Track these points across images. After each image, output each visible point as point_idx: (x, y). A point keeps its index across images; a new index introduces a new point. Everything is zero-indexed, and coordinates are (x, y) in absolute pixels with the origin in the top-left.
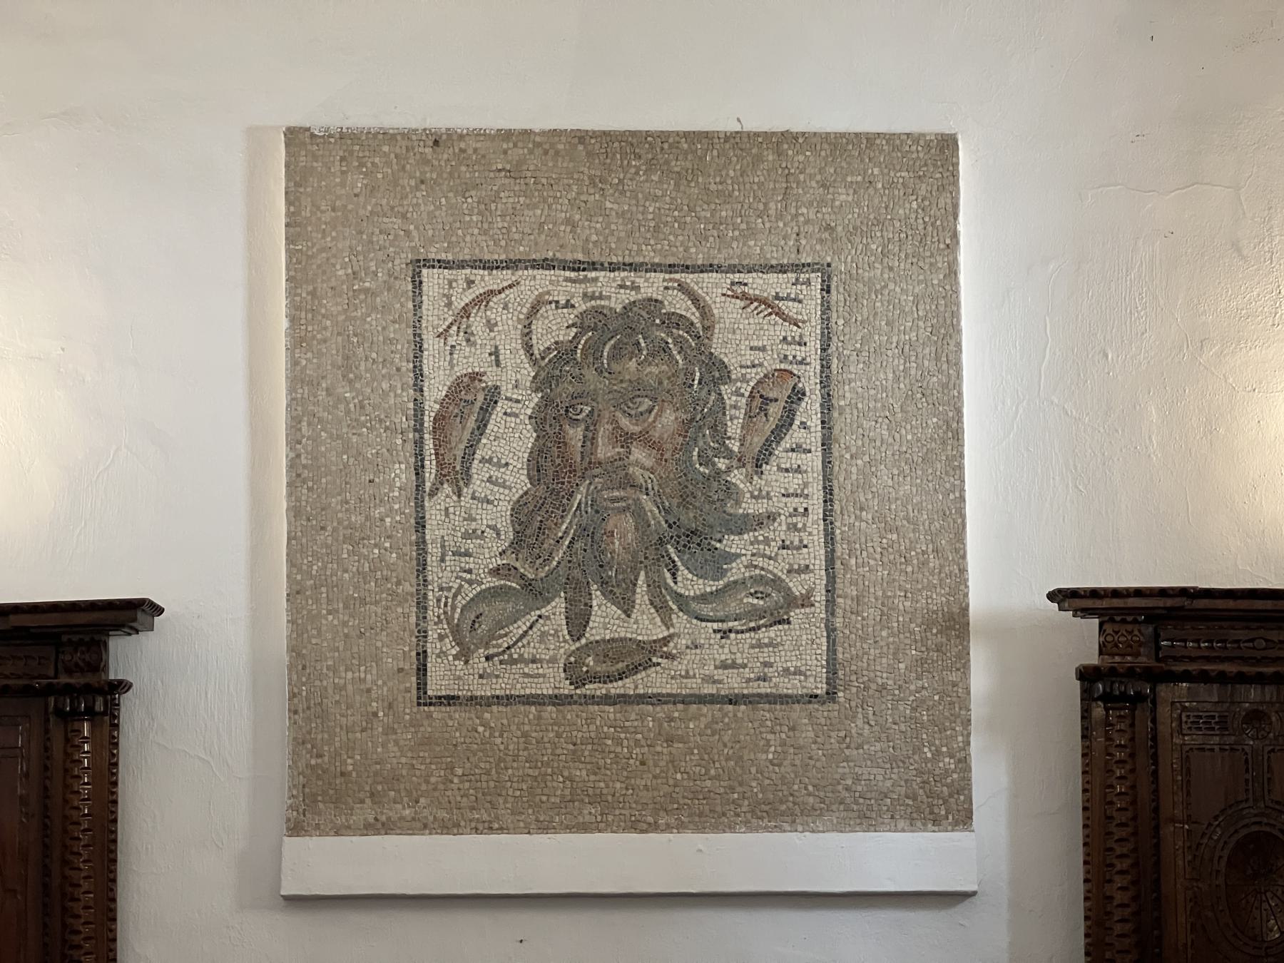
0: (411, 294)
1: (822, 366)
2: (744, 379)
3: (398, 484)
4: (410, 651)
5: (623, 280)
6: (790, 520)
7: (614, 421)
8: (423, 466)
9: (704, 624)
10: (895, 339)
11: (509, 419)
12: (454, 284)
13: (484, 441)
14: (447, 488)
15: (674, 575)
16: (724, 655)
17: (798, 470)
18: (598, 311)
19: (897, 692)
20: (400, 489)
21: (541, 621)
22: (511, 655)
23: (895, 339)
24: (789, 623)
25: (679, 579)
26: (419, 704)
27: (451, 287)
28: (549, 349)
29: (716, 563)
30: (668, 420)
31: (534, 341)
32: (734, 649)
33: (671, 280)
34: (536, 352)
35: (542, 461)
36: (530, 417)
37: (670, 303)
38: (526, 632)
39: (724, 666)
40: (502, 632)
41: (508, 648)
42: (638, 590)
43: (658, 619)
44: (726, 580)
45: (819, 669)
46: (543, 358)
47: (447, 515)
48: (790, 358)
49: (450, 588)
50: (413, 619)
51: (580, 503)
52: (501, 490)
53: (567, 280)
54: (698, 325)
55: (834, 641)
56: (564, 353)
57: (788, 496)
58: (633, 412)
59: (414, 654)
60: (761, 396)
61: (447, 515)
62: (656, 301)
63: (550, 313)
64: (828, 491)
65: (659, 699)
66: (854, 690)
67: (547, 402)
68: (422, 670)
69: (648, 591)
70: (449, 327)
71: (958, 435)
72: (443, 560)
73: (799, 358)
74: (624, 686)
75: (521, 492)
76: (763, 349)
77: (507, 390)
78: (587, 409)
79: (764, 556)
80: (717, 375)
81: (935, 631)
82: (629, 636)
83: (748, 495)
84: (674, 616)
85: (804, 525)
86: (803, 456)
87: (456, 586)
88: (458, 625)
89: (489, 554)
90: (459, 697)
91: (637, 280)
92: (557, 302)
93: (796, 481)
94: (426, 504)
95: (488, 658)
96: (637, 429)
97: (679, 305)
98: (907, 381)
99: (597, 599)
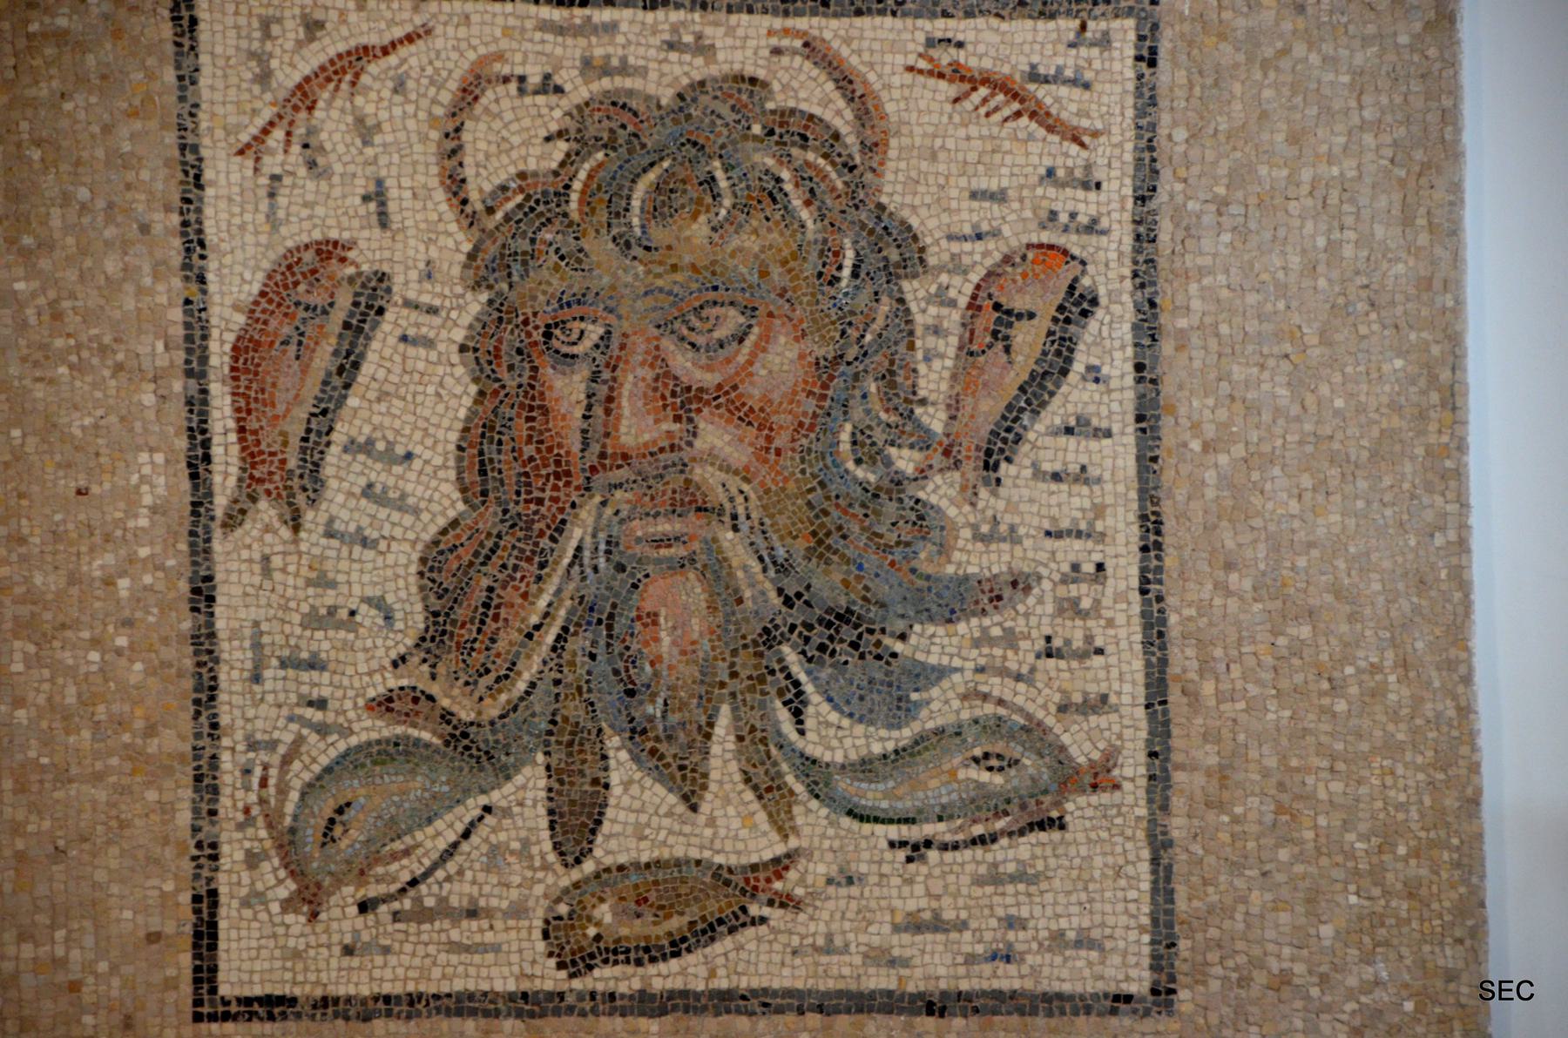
0: (170, 49)
1: (1138, 238)
2: (957, 266)
3: (148, 500)
4: (178, 890)
5: (675, 29)
6: (1062, 591)
7: (657, 358)
8: (207, 458)
9: (867, 828)
10: (1306, 175)
11: (411, 351)
12: (275, 29)
13: (353, 401)
14: (266, 511)
15: (797, 714)
16: (915, 901)
17: (1082, 475)
18: (618, 103)
19: (1315, 992)
20: (154, 510)
21: (489, 819)
22: (418, 900)
23: (1306, 175)
24: (1062, 827)
25: (810, 723)
26: (198, 1018)
27: (267, 35)
28: (504, 188)
29: (898, 689)
30: (780, 364)
31: (469, 172)
32: (937, 887)
33: (786, 32)
34: (474, 196)
35: (490, 450)
36: (463, 349)
37: (785, 87)
38: (455, 845)
39: (915, 925)
40: (398, 846)
41: (414, 883)
42: (715, 749)
43: (761, 817)
44: (916, 727)
45: (1133, 935)
46: (490, 211)
47: (267, 571)
48: (1064, 218)
49: (272, 745)
50: (184, 817)
51: (579, 549)
52: (396, 516)
53: (545, 26)
54: (851, 140)
55: (1169, 868)
56: (539, 202)
57: (1059, 535)
58: (700, 340)
59: (185, 898)
60: (997, 307)
61: (267, 571)
62: (753, 81)
63: (506, 104)
64: (1151, 524)
65: (765, 1002)
66: (1215, 985)
67: (500, 313)
68: (206, 937)
69: (739, 752)
70: (265, 131)
71: (1452, 400)
72: (257, 678)
73: (1083, 219)
74: (683, 972)
75: (442, 522)
76: (999, 197)
77: (406, 284)
78: (595, 332)
79: (1003, 672)
80: (894, 256)
81: (1402, 850)
82: (694, 854)
83: (966, 533)
84: (797, 810)
85: (1097, 602)
86: (1094, 445)
87: (288, 738)
88: (293, 831)
89: (367, 663)
90: (293, 1001)
91: (709, 31)
92: (522, 79)
93: (1076, 502)
94: (217, 546)
95: (363, 907)
96: (710, 379)
97: (804, 89)
98: (1335, 274)
99: (621, 766)
